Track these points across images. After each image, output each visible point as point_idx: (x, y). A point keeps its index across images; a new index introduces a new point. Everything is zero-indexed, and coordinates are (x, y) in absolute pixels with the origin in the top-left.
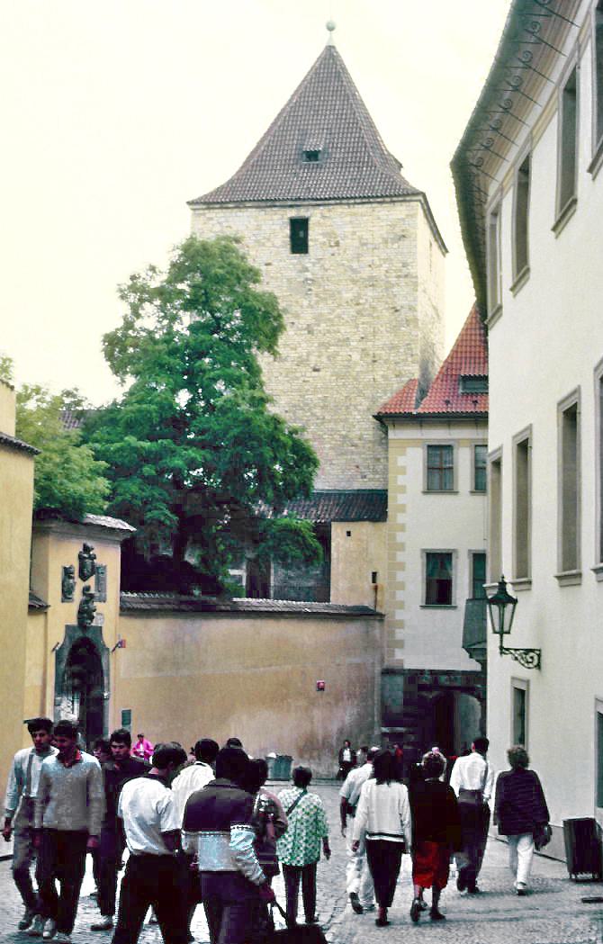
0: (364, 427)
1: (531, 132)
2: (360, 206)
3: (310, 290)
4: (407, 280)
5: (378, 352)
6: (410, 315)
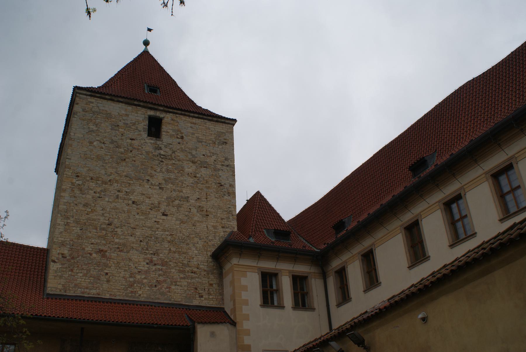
2: (197, 119)
3: (162, 162)
4: (228, 168)
5: (209, 209)
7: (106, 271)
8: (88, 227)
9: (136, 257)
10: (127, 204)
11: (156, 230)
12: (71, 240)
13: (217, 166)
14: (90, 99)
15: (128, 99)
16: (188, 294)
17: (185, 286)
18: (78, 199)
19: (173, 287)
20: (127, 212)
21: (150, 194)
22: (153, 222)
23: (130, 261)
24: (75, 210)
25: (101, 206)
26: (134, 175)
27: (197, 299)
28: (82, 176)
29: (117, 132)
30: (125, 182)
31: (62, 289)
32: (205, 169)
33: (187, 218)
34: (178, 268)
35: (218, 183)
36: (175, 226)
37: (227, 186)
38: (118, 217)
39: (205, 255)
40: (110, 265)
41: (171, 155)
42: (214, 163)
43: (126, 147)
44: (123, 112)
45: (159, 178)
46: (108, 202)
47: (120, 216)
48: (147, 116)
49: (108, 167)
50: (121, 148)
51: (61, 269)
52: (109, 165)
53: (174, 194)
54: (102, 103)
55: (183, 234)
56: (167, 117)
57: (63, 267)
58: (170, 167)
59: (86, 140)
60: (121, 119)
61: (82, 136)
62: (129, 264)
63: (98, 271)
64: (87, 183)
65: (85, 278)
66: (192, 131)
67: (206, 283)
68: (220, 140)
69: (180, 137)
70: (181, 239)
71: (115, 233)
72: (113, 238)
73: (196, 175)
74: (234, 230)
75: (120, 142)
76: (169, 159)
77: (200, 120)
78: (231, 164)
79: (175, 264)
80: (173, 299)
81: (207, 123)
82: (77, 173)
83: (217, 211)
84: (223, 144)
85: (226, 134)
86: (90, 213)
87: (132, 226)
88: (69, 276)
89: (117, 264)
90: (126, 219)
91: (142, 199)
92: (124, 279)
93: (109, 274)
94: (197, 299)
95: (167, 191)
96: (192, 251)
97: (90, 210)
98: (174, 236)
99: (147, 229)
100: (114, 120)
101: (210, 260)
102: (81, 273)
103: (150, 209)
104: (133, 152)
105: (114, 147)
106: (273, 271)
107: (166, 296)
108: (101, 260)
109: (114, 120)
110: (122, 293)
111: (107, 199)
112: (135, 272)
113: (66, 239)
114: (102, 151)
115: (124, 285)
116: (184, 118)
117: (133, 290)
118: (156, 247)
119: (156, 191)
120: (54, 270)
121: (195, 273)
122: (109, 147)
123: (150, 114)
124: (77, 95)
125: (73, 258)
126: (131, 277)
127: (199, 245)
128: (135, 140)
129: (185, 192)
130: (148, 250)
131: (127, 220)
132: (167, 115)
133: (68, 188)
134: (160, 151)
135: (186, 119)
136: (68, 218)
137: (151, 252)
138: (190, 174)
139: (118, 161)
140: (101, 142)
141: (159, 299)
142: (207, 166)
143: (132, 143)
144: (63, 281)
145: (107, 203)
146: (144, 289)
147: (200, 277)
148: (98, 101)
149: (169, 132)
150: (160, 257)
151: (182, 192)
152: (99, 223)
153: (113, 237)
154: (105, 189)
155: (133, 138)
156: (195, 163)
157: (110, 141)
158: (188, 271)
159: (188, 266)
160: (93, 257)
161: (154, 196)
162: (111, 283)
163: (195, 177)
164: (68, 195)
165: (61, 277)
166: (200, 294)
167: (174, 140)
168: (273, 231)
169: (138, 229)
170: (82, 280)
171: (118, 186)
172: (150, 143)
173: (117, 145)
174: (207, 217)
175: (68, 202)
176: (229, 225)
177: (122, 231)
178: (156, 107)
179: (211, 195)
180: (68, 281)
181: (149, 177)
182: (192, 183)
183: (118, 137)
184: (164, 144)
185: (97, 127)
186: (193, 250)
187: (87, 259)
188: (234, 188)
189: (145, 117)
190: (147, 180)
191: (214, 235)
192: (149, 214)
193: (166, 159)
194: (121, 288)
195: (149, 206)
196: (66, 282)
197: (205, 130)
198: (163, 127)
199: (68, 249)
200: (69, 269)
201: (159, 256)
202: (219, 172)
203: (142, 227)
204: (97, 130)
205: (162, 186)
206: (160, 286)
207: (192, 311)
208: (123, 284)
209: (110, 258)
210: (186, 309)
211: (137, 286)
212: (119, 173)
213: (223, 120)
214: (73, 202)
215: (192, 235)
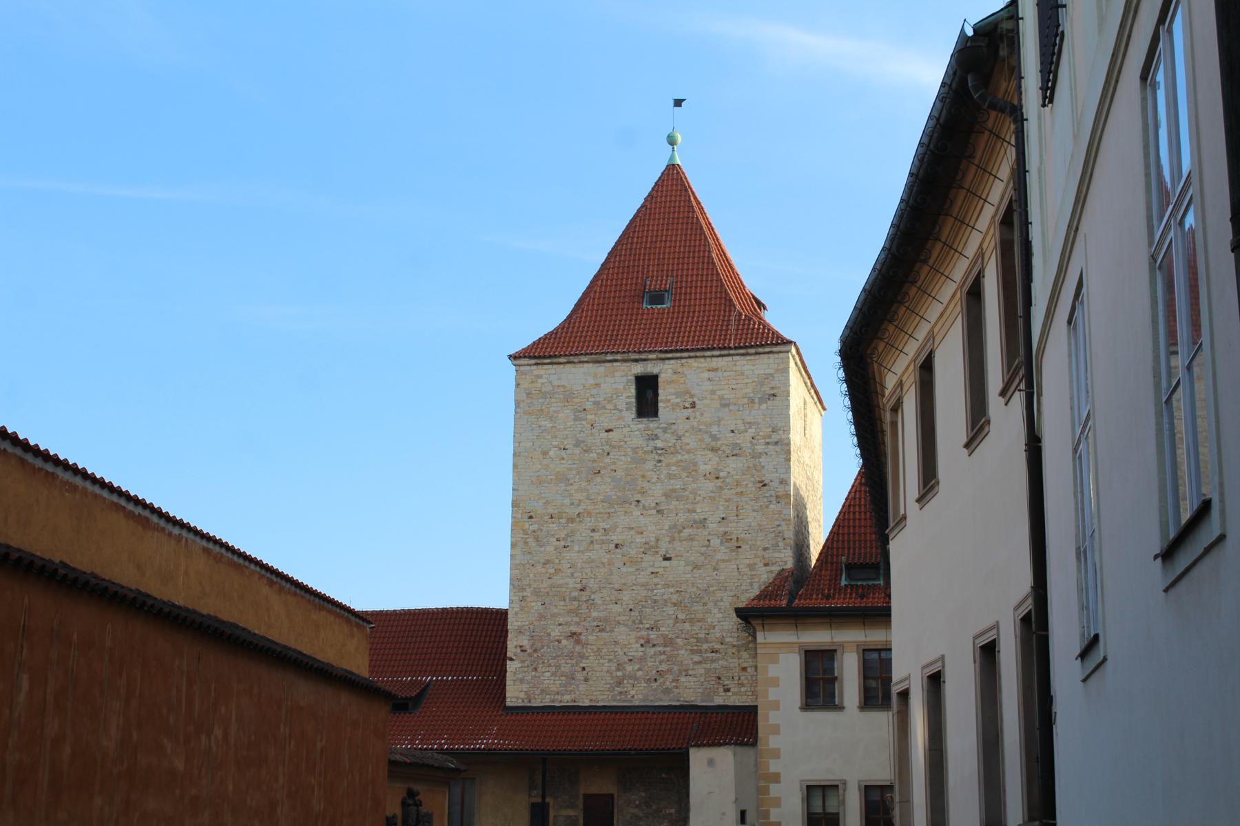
0: (727, 625)
1: (932, 330)
2: (720, 359)
3: (660, 461)
4: (778, 448)
5: (743, 535)
6: (781, 491)
7: (582, 665)
8: (553, 599)
9: (624, 637)
11: (654, 588)
17: (701, 675)
19: (683, 679)
20: (609, 564)
25: (569, 561)
27: (720, 694)
29: (583, 422)
32: (735, 458)
33: (703, 557)
34: (689, 647)
36: (683, 575)
37: (775, 484)
38: (595, 575)
40: (587, 654)
42: (751, 442)
44: (591, 381)
45: (656, 492)
46: (579, 552)
47: (597, 574)
49: (575, 490)
52: (575, 487)
53: (682, 518)
54: (555, 374)
56: (665, 370)
58: (674, 468)
59: (537, 449)
61: (532, 444)
62: (616, 650)
65: (554, 678)
66: (711, 388)
68: (764, 391)
69: (688, 406)
70: (693, 596)
71: (592, 602)
73: (719, 474)
75: (590, 441)
76: (672, 453)
78: (783, 437)
79: (686, 641)
80: (682, 699)
83: (757, 537)
84: (769, 399)
85: (775, 375)
87: (617, 586)
91: (629, 537)
92: (608, 675)
93: (587, 669)
94: (720, 694)
95: (670, 515)
99: (639, 588)
104: (611, 454)
106: (827, 648)
108: (574, 648)
109: (577, 400)
110: (606, 696)
111: (576, 548)
113: (523, 623)
114: (563, 464)
117: (622, 690)
118: (653, 617)
119: (650, 519)
121: (716, 652)
123: (636, 372)
125: (535, 651)
126: (618, 670)
127: (724, 602)
128: (612, 431)
129: (701, 511)
130: (642, 623)
132: (666, 367)
133: (519, 539)
134: (656, 442)
135: (700, 365)
137: (648, 626)
139: (590, 476)
140: (561, 449)
141: (661, 700)
143: (609, 437)
144: (525, 687)
146: (639, 687)
148: (549, 372)
149: (669, 401)
150: (660, 633)
151: (695, 512)
153: (590, 610)
154: (571, 532)
155: (609, 428)
157: (574, 442)
158: (706, 650)
159: (706, 641)
163: (717, 478)
165: (522, 681)
166: (726, 687)
172: (639, 430)
173: (585, 448)
175: (520, 564)
176: (777, 560)
178: (643, 356)
180: (531, 685)
181: (639, 495)
182: (712, 492)
183: (586, 432)
184: (661, 426)
185: (552, 420)
186: (714, 614)
188: (788, 485)
189: (628, 381)
191: (749, 581)
193: (666, 456)
195: (641, 548)
199: (528, 638)
201: (659, 630)
202: (761, 460)
203: (631, 586)
204: (552, 427)
206: (662, 680)
208: (608, 682)
209: (587, 644)
211: (628, 683)
212: (592, 497)
214: (528, 563)
215: (712, 587)
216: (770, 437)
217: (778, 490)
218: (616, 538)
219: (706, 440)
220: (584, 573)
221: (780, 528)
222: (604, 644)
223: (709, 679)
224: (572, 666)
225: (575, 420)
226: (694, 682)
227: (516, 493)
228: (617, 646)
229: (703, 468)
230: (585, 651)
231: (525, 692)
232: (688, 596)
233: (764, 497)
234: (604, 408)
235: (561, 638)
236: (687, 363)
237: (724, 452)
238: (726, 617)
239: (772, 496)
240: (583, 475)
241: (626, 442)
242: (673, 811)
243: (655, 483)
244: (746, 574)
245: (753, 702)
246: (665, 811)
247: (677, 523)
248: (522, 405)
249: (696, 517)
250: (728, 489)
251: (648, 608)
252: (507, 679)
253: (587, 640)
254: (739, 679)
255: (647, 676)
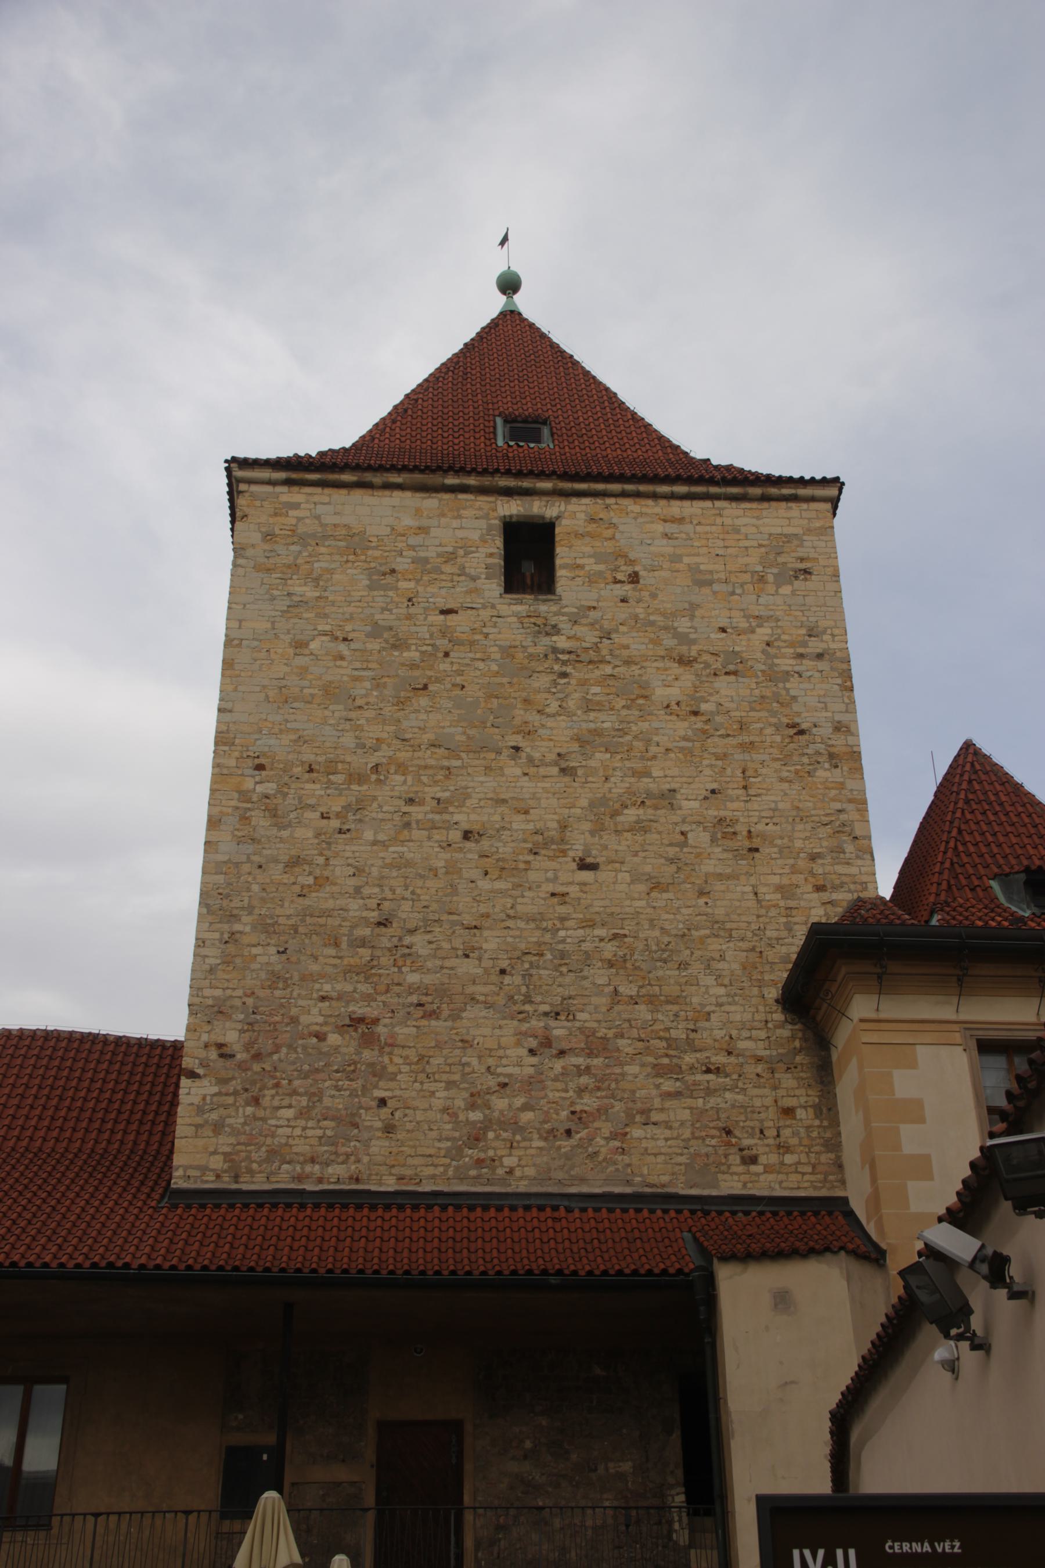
2: (687, 503)
3: (564, 675)
4: (823, 665)
5: (761, 827)
6: (839, 742)
7: (379, 1094)
8: (307, 941)
9: (487, 1031)
10: (444, 844)
11: (559, 925)
12: (249, 992)
13: (776, 661)
14: (287, 495)
15: (422, 471)
16: (697, 1155)
17: (682, 1123)
18: (267, 846)
19: (637, 1132)
20: (447, 873)
21: (527, 796)
22: (545, 899)
23: (464, 1048)
24: (255, 888)
25: (350, 861)
26: (464, 738)
28: (275, 765)
29: (391, 593)
30: (431, 767)
31: (225, 1171)
32: (732, 678)
34: (651, 1059)
35: (788, 726)
36: (628, 903)
37: (826, 730)
38: (413, 893)
39: (754, 1001)
40: (391, 1069)
41: (596, 647)
42: (763, 652)
43: (427, 642)
44: (408, 521)
46: (375, 843)
47: (418, 891)
48: (497, 522)
49: (367, 720)
50: (408, 649)
51: (215, 1099)
52: (370, 714)
53: (618, 786)
54: (329, 503)
55: (662, 928)
57: (223, 1090)
58: (596, 689)
59: (282, 636)
60: (400, 545)
61: (269, 625)
62: (464, 1060)
63: (350, 1096)
64: (293, 786)
65: (302, 1123)
66: (669, 550)
67: (767, 1108)
70: (654, 948)
71: (407, 951)
72: (400, 971)
74: (862, 895)
76: (590, 662)
77: (699, 504)
78: (833, 646)
80: (638, 1179)
81: (726, 512)
82: (258, 757)
85: (805, 538)
86: (311, 891)
87: (468, 919)
88: (245, 1124)
89: (417, 1063)
90: (444, 899)
92: (446, 1117)
93: (390, 1103)
94: (734, 1169)
95: (590, 779)
96: (703, 989)
97: (310, 880)
98: (626, 940)
99: (521, 924)
100: (377, 553)
101: (779, 1016)
102: (290, 1106)
103: (531, 850)
104: (452, 654)
105: (384, 649)
107: (611, 1169)
108: (358, 1053)
109: (377, 553)
110: (441, 1169)
111: (369, 835)
112: (489, 1088)
113: (229, 992)
115: (448, 1139)
116: (630, 505)
117: (482, 1155)
119: (548, 785)
120: (192, 1104)
122: (364, 651)
123: (507, 513)
124: (243, 487)
125: (257, 1057)
126: (472, 1107)
127: (729, 962)
128: (456, 612)
129: (661, 773)
130: (531, 1002)
131: (448, 899)
132: (571, 508)
133: (230, 810)
134: (554, 638)
135: (644, 510)
136: (233, 917)
137: (546, 1008)
138: (675, 707)
139: (402, 694)
140: (337, 638)
141: (583, 1180)
142: (740, 667)
143: (449, 624)
144: (225, 1142)
145: (369, 848)
146: (526, 1148)
147: (740, 1084)
148: (316, 499)
149: (581, 567)
150: (578, 1024)
151: (647, 774)
152: (344, 924)
153: (400, 968)
156: (690, 662)
157: (369, 628)
158: (692, 1067)
159: (691, 1046)
160: (328, 1046)
161: (544, 803)
162: (399, 1137)
163: (696, 713)
164: (229, 838)
165: (218, 1128)
166: (745, 1152)
167: (603, 593)
168: (1023, 877)
169: (488, 928)
170: (295, 1134)
171: (405, 782)
172: (515, 614)
173: (392, 641)
174: (751, 855)
175: (229, 861)
176: (845, 879)
177: (430, 942)
178: (526, 484)
179: (764, 771)
180: (243, 1138)
181: (519, 738)
182: (685, 739)
183: (394, 611)
184: (566, 610)
186: (707, 987)
187: (310, 1054)
188: (852, 734)
189: (490, 528)
190: (513, 748)
191: (784, 920)
192: (526, 870)
194: (439, 1148)
195: (525, 841)
196: (239, 1144)
197: (721, 536)
198: (559, 550)
199: (239, 1026)
200: (245, 1095)
201: (574, 1018)
202: (788, 685)
203: (503, 921)
205: (572, 764)
206: (583, 1134)
207: (713, 1219)
208: (445, 1134)
209: (391, 1045)
210: (693, 1212)
211: (497, 1137)
212: (407, 736)
213: (786, 491)
214: (249, 860)
215: (697, 929)
216: (805, 644)
217: (831, 742)
218: (463, 818)
219: (665, 642)
220: (386, 889)
221: (843, 817)
222: (436, 1046)
223: (703, 1134)
224: (353, 1094)
225: (371, 588)
226: (666, 1140)
227: (228, 717)
228: (469, 1051)
229: (660, 693)
230: (386, 1059)
231: (224, 1154)
232: (640, 945)
233: (804, 754)
234: (438, 571)
235: (325, 1029)
236: (617, 504)
237: (707, 665)
238: (736, 995)
239: (818, 753)
240: (388, 692)
241: (486, 635)
242: (627, 1467)
243: (554, 716)
244: (776, 906)
245: (815, 1188)
246: (607, 1469)
247: (608, 796)
248: (250, 552)
249: (651, 785)
250: (719, 736)
251: (545, 968)
252: (179, 1121)
253: (393, 1036)
254: (778, 1136)
255: (545, 1122)
